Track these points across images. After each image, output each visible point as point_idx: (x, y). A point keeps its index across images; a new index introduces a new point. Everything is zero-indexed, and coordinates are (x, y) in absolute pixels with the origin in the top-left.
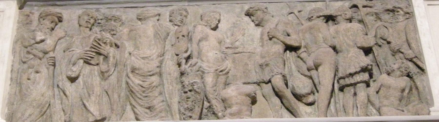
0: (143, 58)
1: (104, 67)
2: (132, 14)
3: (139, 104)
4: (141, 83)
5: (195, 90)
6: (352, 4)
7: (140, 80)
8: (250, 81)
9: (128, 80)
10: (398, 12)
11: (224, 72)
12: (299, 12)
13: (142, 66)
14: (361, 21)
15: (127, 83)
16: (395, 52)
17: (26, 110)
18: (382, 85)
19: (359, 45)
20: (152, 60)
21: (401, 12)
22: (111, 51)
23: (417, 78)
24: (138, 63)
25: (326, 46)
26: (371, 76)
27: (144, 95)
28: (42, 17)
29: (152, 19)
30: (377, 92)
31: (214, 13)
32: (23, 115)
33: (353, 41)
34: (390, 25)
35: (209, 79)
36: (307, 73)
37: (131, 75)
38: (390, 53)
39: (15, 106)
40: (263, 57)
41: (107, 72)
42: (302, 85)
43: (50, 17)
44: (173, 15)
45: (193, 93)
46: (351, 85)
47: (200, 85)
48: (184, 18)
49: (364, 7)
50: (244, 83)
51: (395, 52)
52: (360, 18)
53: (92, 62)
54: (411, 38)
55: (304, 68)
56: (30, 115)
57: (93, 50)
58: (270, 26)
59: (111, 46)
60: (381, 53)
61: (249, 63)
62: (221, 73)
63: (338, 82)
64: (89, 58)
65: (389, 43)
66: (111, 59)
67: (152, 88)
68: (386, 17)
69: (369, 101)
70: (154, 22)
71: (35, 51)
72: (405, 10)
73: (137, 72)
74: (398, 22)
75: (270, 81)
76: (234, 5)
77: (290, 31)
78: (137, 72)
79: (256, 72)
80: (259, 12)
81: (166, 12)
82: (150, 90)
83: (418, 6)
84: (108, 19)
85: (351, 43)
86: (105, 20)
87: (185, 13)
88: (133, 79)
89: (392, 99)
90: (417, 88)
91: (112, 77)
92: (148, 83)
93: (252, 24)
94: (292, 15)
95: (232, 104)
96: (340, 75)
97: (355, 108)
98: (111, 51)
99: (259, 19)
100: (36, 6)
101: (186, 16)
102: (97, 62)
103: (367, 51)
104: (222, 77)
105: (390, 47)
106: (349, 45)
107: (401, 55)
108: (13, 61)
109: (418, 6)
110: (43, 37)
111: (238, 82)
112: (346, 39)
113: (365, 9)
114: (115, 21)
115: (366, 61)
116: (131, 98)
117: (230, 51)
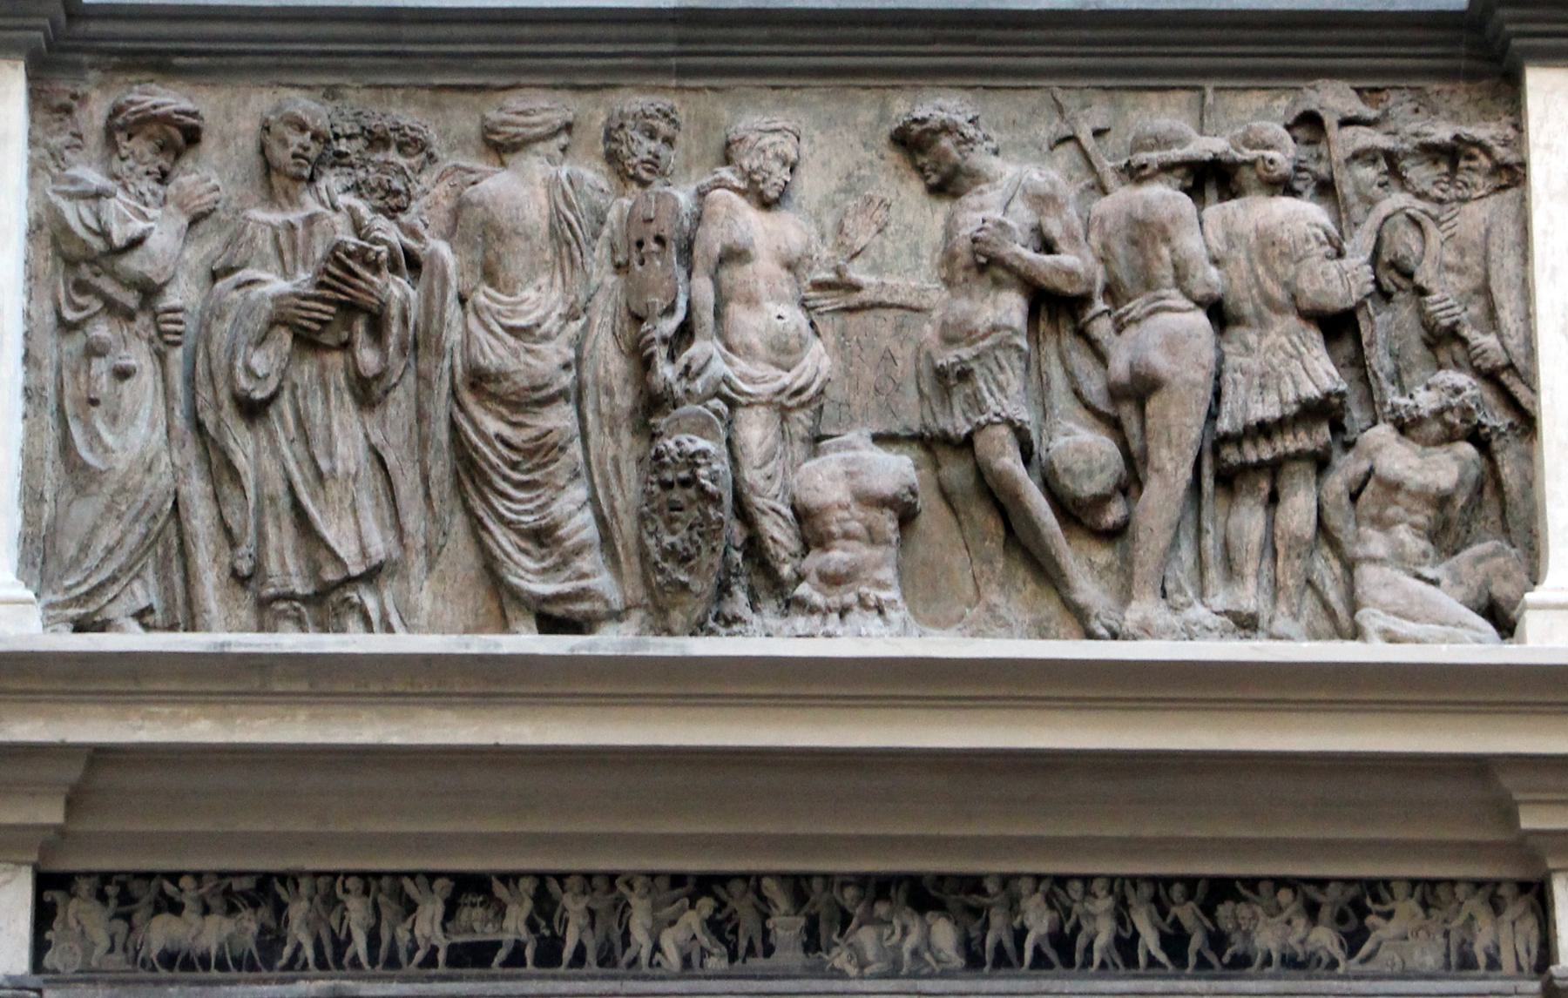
0: (513, 331)
1: (368, 358)
2: (464, 118)
3: (501, 518)
4: (507, 431)
5: (702, 488)
6: (1299, 110)
7: (502, 418)
8: (897, 427)
9: (461, 418)
10: (1471, 157)
11: (805, 397)
12: (1098, 133)
13: (511, 364)
14: (1326, 189)
15: (454, 427)
16: (1442, 340)
17: (94, 529)
18: (1370, 473)
19: (1305, 305)
20: (547, 337)
21: (1484, 161)
22: (396, 289)
23: (1503, 449)
24: (495, 353)
25: (1183, 303)
26: (1337, 428)
27: (517, 476)
28: (120, 127)
29: (540, 147)
30: (1354, 497)
31: (777, 138)
32: (84, 548)
33: (1286, 285)
34: (1434, 209)
35: (755, 431)
36: (1103, 405)
37: (468, 398)
38: (1415, 336)
39: (47, 511)
40: (950, 339)
41: (378, 377)
42: (1083, 449)
43: (154, 129)
44: (621, 135)
45: (691, 492)
46: (1260, 466)
47: (722, 466)
48: (663, 151)
49: (1346, 122)
50: (880, 439)
51: (1442, 340)
52: (1322, 169)
53: (328, 339)
54: (1503, 281)
55: (1094, 387)
56: (110, 551)
57: (328, 293)
58: (980, 211)
59: (394, 269)
60: (1387, 330)
61: (898, 353)
62: (793, 402)
63: (1216, 452)
64: (316, 327)
65: (1421, 292)
66: (395, 328)
67: (543, 451)
68: (1421, 174)
69: (1321, 525)
70: (550, 159)
71: (110, 287)
72: (1500, 152)
73: (492, 387)
74: (1464, 200)
75: (967, 443)
76: (851, 92)
77: (1054, 228)
78: (492, 387)
79: (920, 392)
80: (946, 142)
81: (593, 112)
82: (536, 460)
83: (1548, 147)
84: (377, 140)
85: (1279, 294)
86: (359, 144)
87: (663, 126)
88: (478, 412)
89: (1403, 533)
90: (1498, 485)
91: (398, 393)
92: (533, 433)
93: (916, 187)
94: (1070, 146)
95: (831, 536)
96: (1224, 425)
97: (1268, 552)
98: (396, 289)
99: (945, 169)
100: (92, 66)
101: (669, 141)
102: (345, 335)
103: (1337, 327)
104: (799, 414)
105: (1420, 310)
106: (1269, 301)
107: (1457, 348)
108: (28, 316)
109: (1548, 147)
110: (138, 226)
111: (851, 436)
112: (1260, 270)
113: (1349, 131)
114: (401, 148)
115: (1318, 371)
116: (469, 487)
117: (828, 302)
